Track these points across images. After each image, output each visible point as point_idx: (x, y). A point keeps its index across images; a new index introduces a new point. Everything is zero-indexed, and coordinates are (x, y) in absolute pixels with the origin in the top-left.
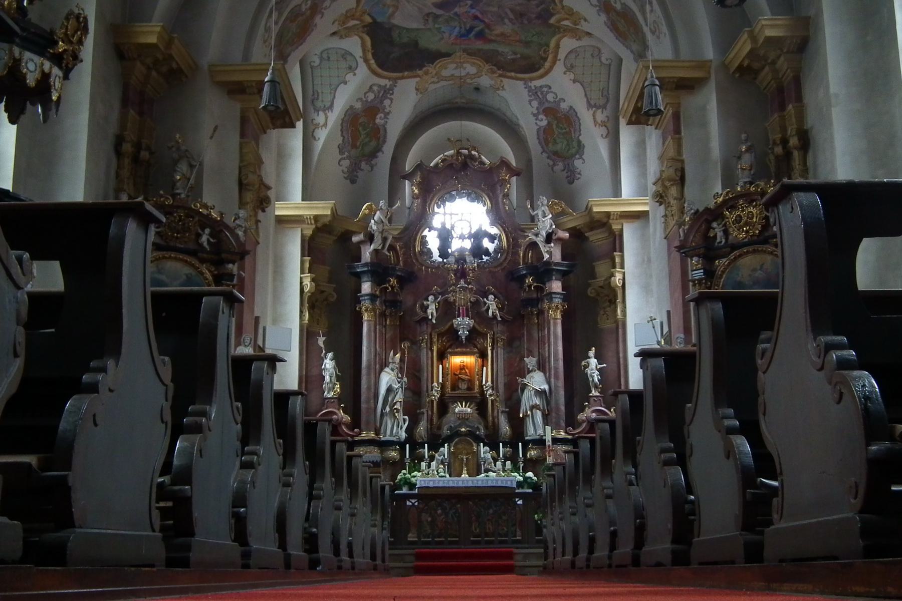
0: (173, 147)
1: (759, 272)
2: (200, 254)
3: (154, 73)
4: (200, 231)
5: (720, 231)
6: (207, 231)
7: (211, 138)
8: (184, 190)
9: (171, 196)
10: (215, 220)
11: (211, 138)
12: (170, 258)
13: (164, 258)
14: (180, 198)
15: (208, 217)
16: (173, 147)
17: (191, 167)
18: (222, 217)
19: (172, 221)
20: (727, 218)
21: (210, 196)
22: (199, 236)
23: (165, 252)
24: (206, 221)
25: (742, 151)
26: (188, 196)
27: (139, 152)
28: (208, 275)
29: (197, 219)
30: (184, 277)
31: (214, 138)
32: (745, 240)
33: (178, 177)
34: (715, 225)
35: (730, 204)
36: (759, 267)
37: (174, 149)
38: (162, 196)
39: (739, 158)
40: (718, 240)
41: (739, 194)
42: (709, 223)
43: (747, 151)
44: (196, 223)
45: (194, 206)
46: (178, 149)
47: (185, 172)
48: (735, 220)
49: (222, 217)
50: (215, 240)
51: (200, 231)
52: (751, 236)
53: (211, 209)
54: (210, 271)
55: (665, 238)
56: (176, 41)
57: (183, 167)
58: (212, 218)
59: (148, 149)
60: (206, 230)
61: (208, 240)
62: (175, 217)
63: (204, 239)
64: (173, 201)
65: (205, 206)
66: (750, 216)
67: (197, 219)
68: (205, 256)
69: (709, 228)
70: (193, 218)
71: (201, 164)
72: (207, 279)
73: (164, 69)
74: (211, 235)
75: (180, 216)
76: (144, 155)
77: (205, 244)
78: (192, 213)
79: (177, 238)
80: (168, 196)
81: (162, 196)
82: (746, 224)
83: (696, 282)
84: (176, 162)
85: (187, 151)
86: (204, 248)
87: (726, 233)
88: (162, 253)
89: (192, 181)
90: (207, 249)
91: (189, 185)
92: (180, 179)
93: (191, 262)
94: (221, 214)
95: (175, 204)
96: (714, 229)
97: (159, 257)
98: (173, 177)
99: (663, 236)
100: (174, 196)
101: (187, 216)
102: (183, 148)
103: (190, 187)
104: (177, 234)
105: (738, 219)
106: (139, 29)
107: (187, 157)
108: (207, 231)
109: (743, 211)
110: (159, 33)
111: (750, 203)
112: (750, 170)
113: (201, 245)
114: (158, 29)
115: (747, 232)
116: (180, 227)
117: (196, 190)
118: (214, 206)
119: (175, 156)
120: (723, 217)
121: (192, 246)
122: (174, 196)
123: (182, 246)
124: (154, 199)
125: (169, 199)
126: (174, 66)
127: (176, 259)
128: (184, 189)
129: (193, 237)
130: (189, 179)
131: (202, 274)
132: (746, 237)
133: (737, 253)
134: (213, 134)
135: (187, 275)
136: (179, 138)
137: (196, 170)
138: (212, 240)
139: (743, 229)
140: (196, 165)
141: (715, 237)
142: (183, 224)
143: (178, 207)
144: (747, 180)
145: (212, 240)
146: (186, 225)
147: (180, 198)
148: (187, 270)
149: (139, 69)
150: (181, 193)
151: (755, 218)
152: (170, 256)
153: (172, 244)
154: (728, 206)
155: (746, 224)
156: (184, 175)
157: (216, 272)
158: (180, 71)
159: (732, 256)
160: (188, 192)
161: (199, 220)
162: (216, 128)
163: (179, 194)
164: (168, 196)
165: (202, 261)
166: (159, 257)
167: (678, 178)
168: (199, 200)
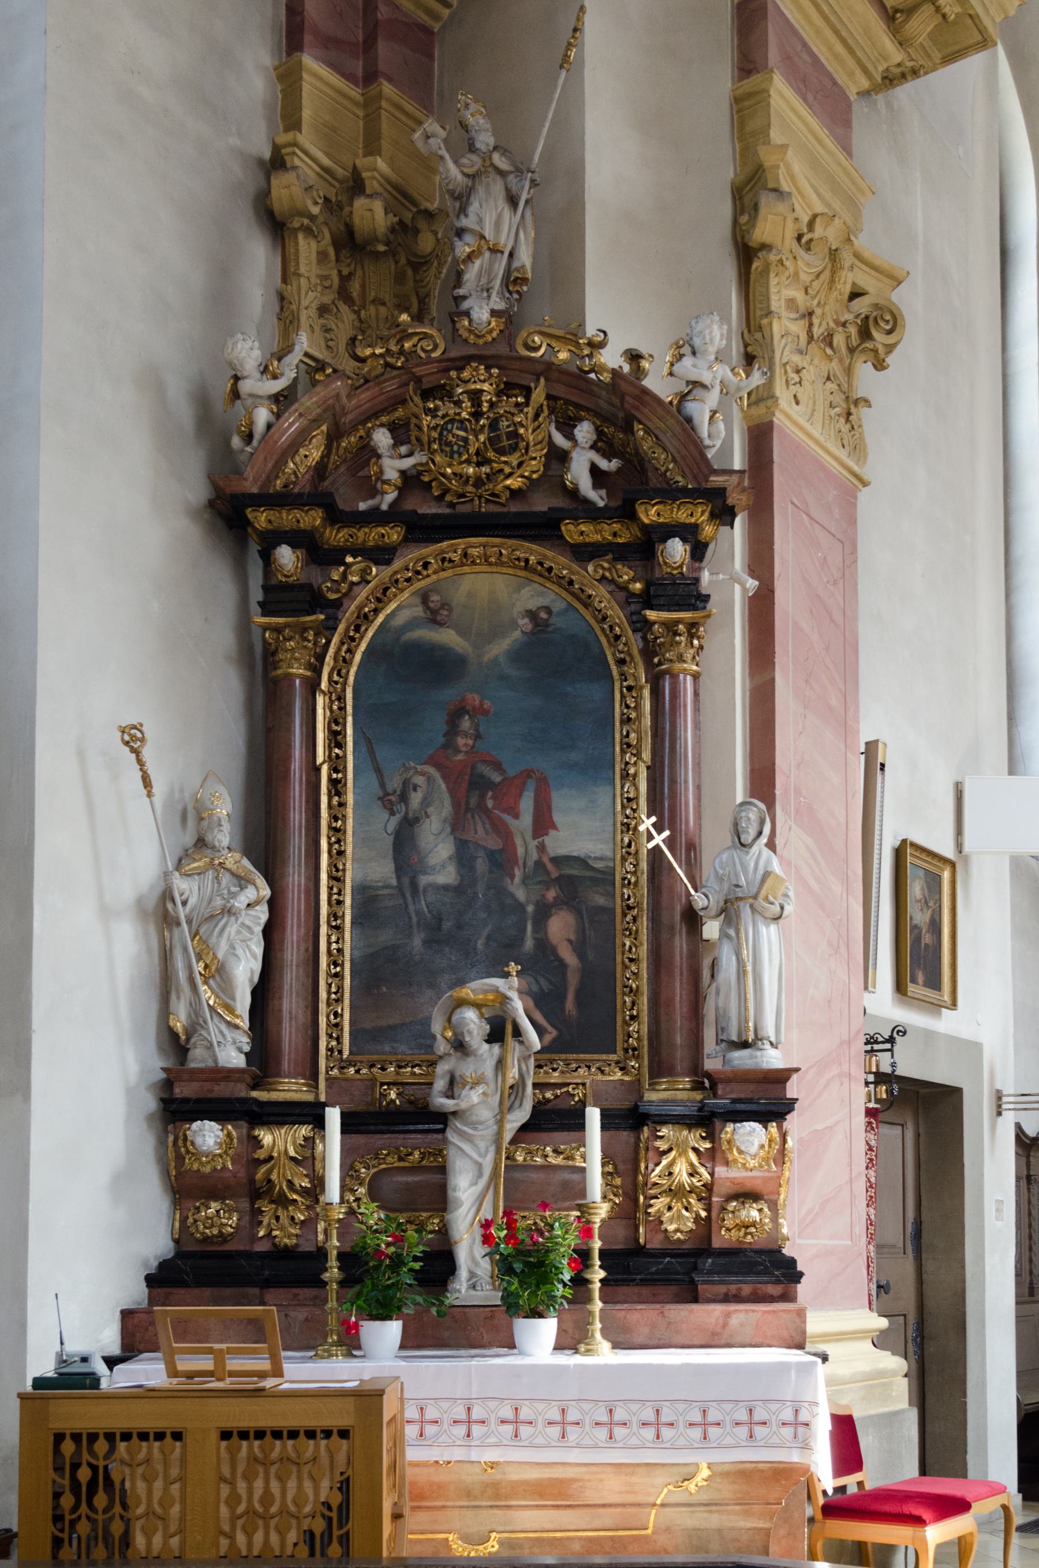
6: (584, 431)
18: (639, 372)
22: (559, 458)
29: (539, 395)
30: (525, 623)
51: (559, 439)
61: (594, 470)
67: (539, 395)
74: (603, 445)
101: (506, 389)
108: (584, 431)
113: (573, 493)
135: (532, 615)
138: (603, 464)
142: (494, 425)
146: (504, 423)
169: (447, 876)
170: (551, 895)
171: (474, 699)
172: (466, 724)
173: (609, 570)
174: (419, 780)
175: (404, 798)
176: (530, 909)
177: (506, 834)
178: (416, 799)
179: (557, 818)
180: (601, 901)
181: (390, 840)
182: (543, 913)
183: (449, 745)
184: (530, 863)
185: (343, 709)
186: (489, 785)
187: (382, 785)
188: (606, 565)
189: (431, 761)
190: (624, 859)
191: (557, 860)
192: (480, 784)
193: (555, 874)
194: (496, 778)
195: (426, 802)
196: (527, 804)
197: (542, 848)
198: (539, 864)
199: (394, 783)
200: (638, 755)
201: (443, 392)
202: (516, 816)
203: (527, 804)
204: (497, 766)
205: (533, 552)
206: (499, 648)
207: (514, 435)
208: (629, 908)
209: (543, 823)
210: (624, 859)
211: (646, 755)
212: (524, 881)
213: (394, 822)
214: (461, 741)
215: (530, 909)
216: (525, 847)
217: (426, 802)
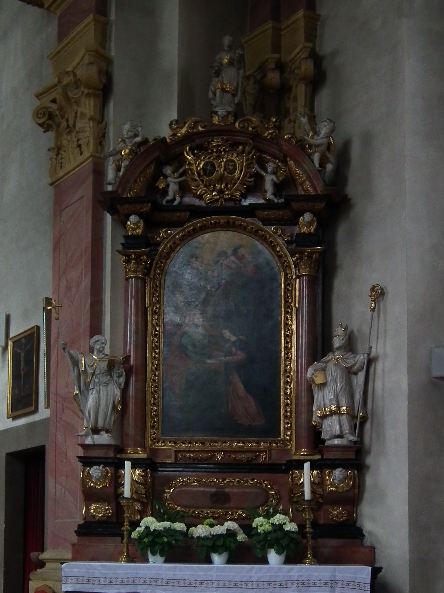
1: (233, 258)
5: (175, 183)
20: (190, 164)
25: (222, 64)
32: (215, 205)
34: (168, 170)
35: (198, 141)
36: (230, 252)
39: (218, 73)
40: (169, 197)
41: (215, 128)
42: (160, 165)
43: (231, 63)
48: (204, 169)
52: (226, 200)
55: (52, 184)
66: (230, 167)
69: (158, 174)
82: (221, 179)
83: (133, 256)
87: (184, 188)
96: (166, 177)
99: (50, 181)
105: (209, 167)
109: (219, 157)
111: (234, 145)
112: (234, 95)
115: (221, 192)
120: (181, 161)
132: (217, 200)
133: (198, 222)
139: (215, 187)
141: (165, 191)
144: (230, 109)
151: (237, 172)
154: (194, 145)
155: (221, 179)
159: (189, 226)
167: (101, 86)
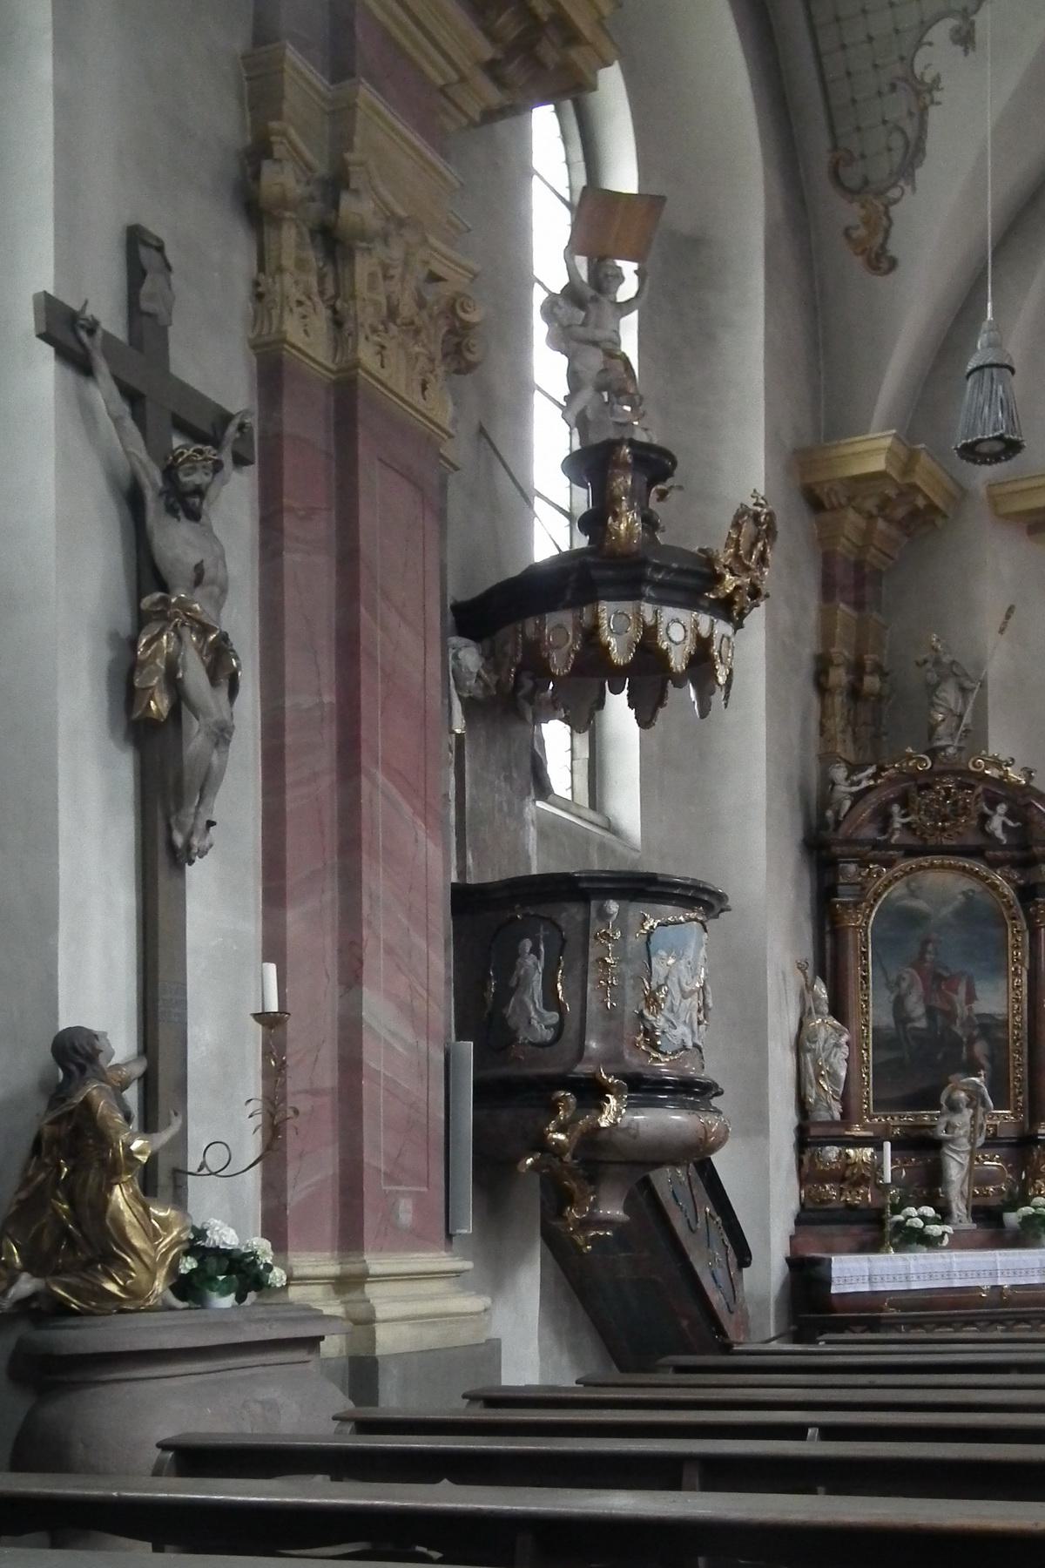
0: (925, 662)
2: (989, 854)
3: (881, 524)
4: (986, 809)
6: (1002, 808)
7: (1001, 631)
8: (953, 739)
9: (926, 753)
10: (1016, 786)
11: (1001, 631)
12: (932, 866)
13: (921, 868)
14: (945, 756)
15: (1001, 782)
16: (925, 662)
17: (964, 691)
18: (1029, 777)
19: (932, 800)
21: (998, 746)
22: (985, 818)
23: (921, 859)
24: (999, 791)
26: (960, 749)
27: (861, 680)
28: (1008, 890)
29: (980, 789)
30: (960, 897)
31: (1007, 632)
33: (940, 717)
37: (929, 666)
38: (910, 757)
44: (978, 796)
45: (974, 766)
46: (937, 662)
47: (952, 706)
49: (1029, 777)
50: (1018, 824)
51: (986, 809)
53: (1008, 765)
54: (1009, 880)
56: (924, 458)
57: (949, 695)
58: (1010, 784)
59: (879, 670)
60: (998, 808)
61: (1004, 825)
62: (939, 793)
63: (996, 824)
64: (933, 762)
65: (997, 763)
67: (980, 789)
68: (999, 853)
70: (972, 787)
71: (983, 685)
72: (1005, 896)
73: (900, 512)
74: (1010, 814)
75: (948, 790)
76: (871, 683)
77: (999, 833)
78: (970, 779)
79: (943, 829)
80: (922, 756)
81: (910, 757)
84: (932, 689)
85: (953, 662)
86: (998, 840)
88: (915, 860)
89: (967, 719)
90: (1001, 841)
91: (962, 728)
92: (943, 720)
93: (972, 869)
94: (1028, 773)
95: (937, 767)
97: (911, 869)
98: (930, 716)
100: (933, 753)
101: (961, 786)
102: (946, 659)
103: (964, 732)
104: (943, 822)
106: (850, 450)
107: (955, 675)
108: (1002, 808)
110: (889, 449)
113: (991, 836)
114: (888, 442)
116: (948, 810)
117: (975, 736)
118: (1013, 760)
119: (932, 677)
121: (972, 840)
122: (933, 753)
123: (954, 843)
124: (896, 765)
125: (924, 760)
126: (921, 502)
127: (942, 866)
128: (952, 736)
129: (974, 822)
130: (961, 717)
131: (994, 887)
134: (1005, 623)
135: (964, 893)
136: (938, 640)
137: (974, 695)
138: (1010, 823)
140: (970, 684)
142: (955, 803)
143: (943, 773)
145: (1010, 823)
146: (961, 803)
147: (945, 756)
148: (966, 884)
149: (852, 520)
150: (949, 746)
152: (932, 864)
153: (932, 841)
156: (951, 710)
157: (1022, 882)
158: (932, 508)
160: (960, 740)
161: (985, 791)
162: (1011, 609)
163: (943, 748)
164: (922, 756)
165: (994, 864)
166: (911, 869)
168: (984, 752)
169: (922, 1024)
170: (976, 1033)
171: (934, 936)
172: (930, 947)
173: (1008, 873)
174: (906, 976)
175: (898, 984)
176: (965, 1039)
177: (951, 1002)
178: (904, 985)
179: (978, 994)
180: (1001, 1035)
181: (891, 1005)
182: (972, 1041)
183: (922, 957)
184: (965, 1018)
185: (867, 940)
186: (945, 979)
187: (887, 979)
188: (1007, 870)
189: (913, 966)
190: (1014, 1016)
191: (979, 1016)
192: (938, 978)
193: (977, 1022)
194: (946, 974)
195: (910, 986)
196: (962, 989)
197: (970, 1009)
198: (969, 1018)
199: (893, 977)
200: (1022, 965)
201: (928, 787)
202: (957, 993)
203: (962, 989)
204: (946, 968)
205: (966, 863)
206: (946, 911)
207: (965, 808)
208: (1018, 1039)
209: (971, 997)
210: (1014, 1016)
211: (1027, 964)
212: (963, 1025)
213: (893, 997)
214: (928, 957)
215: (965, 1039)
216: (961, 1010)
217: (910, 986)
